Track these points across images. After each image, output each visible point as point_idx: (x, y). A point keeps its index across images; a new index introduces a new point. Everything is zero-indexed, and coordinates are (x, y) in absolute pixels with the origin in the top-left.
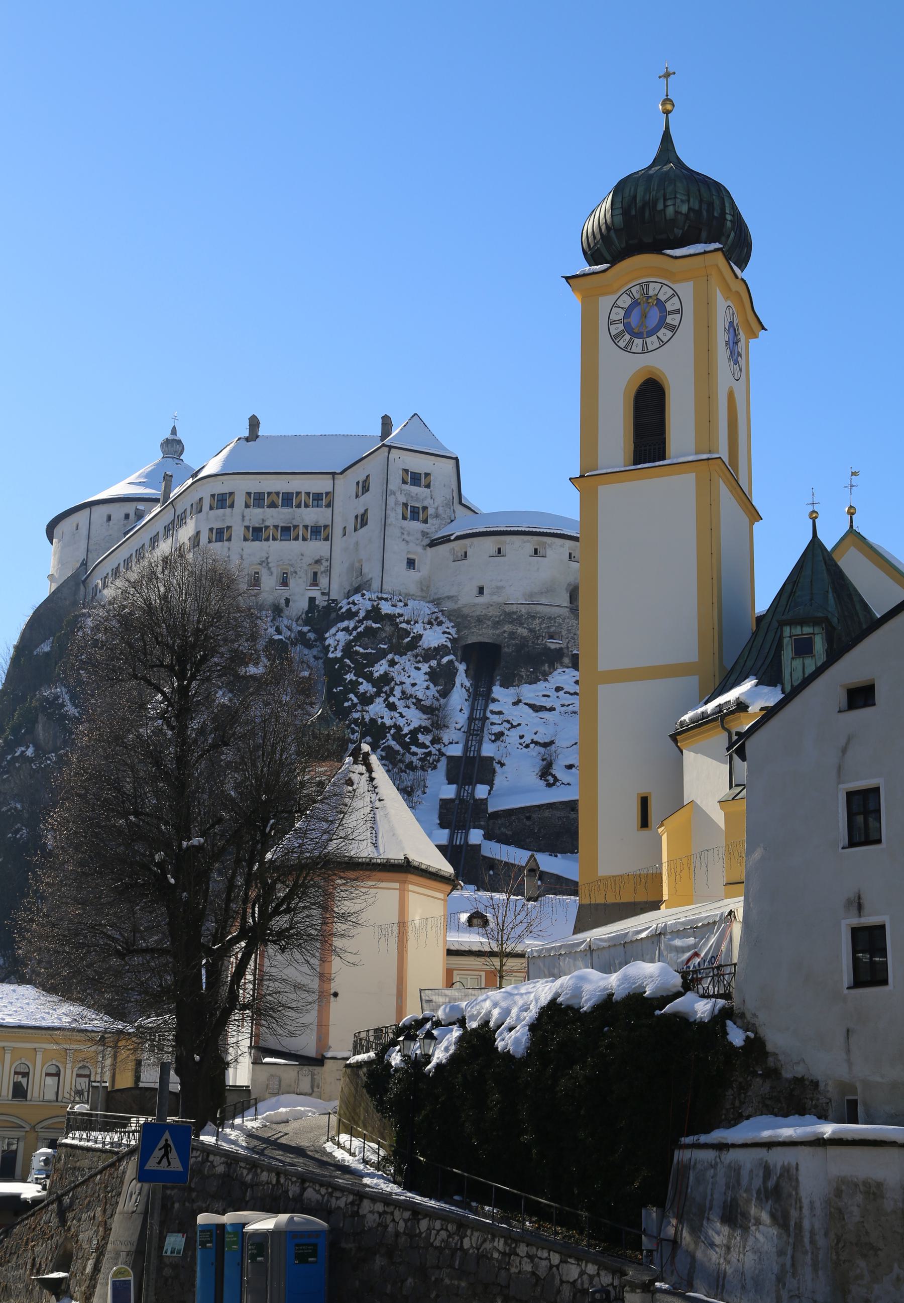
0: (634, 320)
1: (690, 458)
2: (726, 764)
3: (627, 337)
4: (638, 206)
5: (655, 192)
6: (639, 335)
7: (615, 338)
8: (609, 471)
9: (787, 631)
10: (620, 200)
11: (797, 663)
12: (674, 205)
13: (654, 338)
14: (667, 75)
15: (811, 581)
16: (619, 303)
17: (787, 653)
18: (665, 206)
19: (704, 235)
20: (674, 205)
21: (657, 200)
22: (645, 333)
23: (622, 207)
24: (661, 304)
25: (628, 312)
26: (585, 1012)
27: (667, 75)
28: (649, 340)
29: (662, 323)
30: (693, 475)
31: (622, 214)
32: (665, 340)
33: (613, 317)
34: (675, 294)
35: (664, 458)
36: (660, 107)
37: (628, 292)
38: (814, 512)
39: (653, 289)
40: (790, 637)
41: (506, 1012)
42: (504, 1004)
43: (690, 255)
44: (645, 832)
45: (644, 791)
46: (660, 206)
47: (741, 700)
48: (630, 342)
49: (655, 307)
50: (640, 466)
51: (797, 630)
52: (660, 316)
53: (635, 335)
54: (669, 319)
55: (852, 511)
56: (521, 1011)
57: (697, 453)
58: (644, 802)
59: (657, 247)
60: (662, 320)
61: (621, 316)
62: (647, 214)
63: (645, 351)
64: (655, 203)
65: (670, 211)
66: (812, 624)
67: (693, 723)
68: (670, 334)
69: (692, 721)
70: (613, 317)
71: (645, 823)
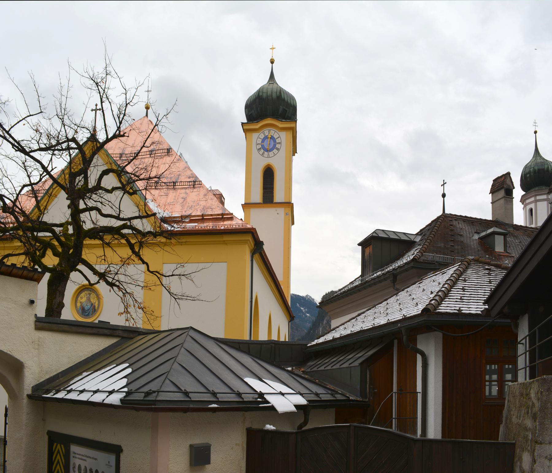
0: (266, 144)
14: (273, 49)
16: (260, 136)
25: (263, 140)
27: (273, 49)
28: (270, 153)
33: (258, 142)
37: (264, 133)
48: (263, 153)
52: (274, 144)
60: (275, 146)
61: (260, 142)
63: (269, 157)
68: (277, 151)
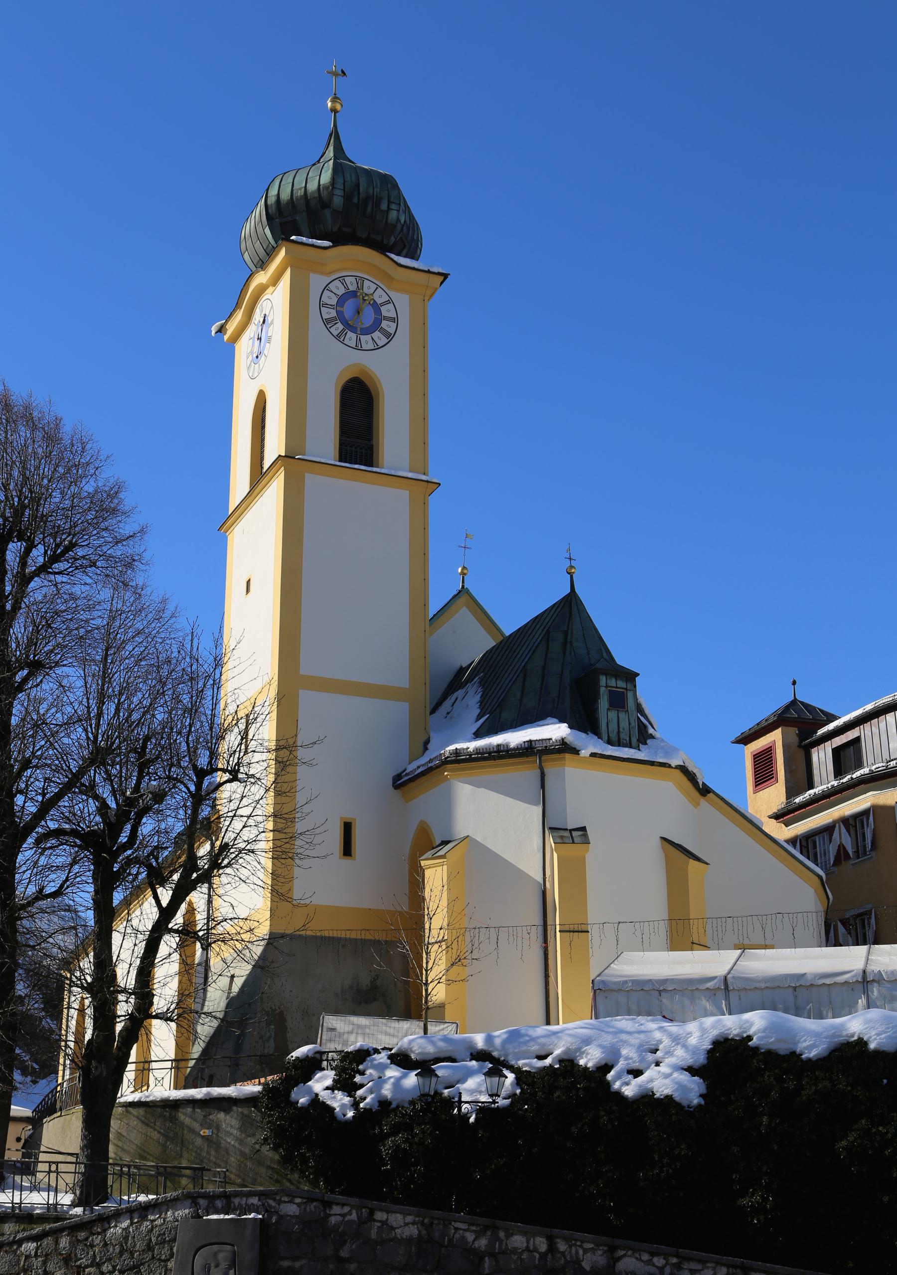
0: (348, 308)
1: (410, 475)
2: (536, 804)
3: (340, 326)
4: (361, 196)
5: (378, 190)
6: (353, 329)
7: (327, 322)
8: (323, 460)
9: (603, 680)
10: (342, 182)
11: (613, 715)
12: (398, 211)
13: (368, 337)
15: (584, 635)
17: (603, 703)
18: (389, 209)
19: (404, 252)
20: (398, 211)
21: (381, 199)
22: (359, 329)
23: (344, 190)
24: (376, 307)
25: (342, 300)
26: (809, 1060)
28: (363, 338)
29: (376, 326)
30: (405, 494)
31: (344, 197)
32: (380, 345)
33: (325, 299)
34: (390, 301)
35: (371, 466)
36: (329, 104)
37: (342, 279)
38: (572, 567)
39: (368, 288)
40: (606, 687)
41: (614, 1053)
42: (607, 1040)
43: (414, 269)
44: (347, 861)
45: (348, 816)
46: (384, 206)
47: (565, 740)
49: (370, 307)
50: (356, 466)
51: (612, 682)
52: (375, 318)
53: (348, 326)
54: (384, 324)
55: (465, 571)
56: (642, 1051)
57: (411, 471)
58: (348, 828)
59: (382, 248)
62: (369, 209)
63: (358, 347)
64: (379, 201)
65: (393, 215)
66: (625, 679)
67: (477, 753)
68: (385, 340)
69: (478, 751)
70: (325, 299)
71: (347, 851)
